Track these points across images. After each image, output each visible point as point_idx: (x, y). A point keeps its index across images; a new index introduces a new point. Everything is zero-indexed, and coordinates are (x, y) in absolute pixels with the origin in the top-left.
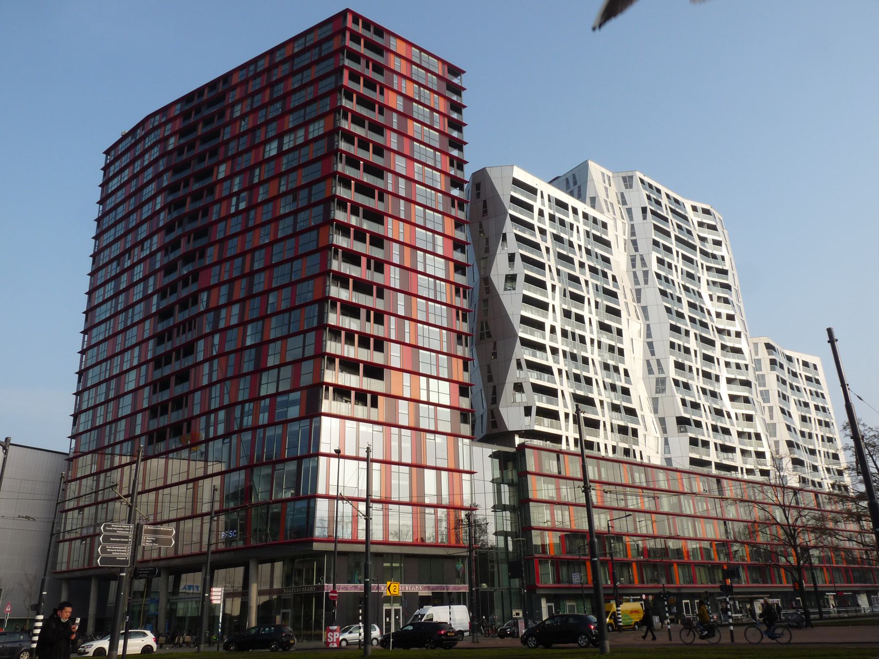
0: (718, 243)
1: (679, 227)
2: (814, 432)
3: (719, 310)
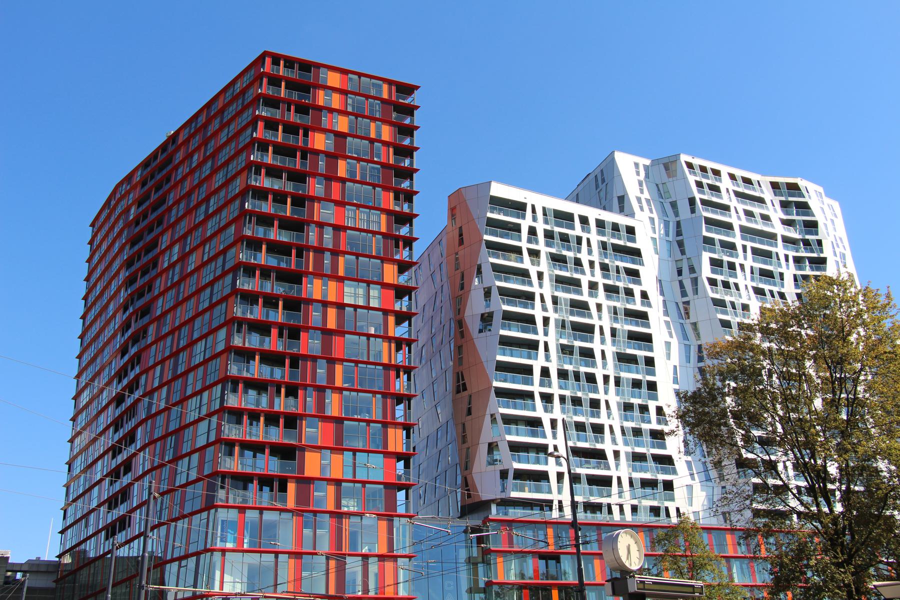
1: (749, 214)
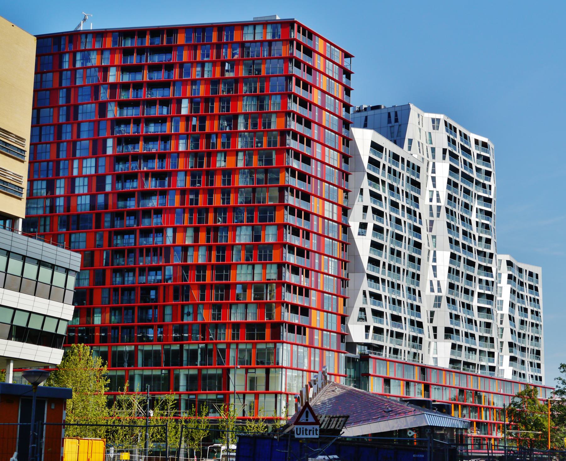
2: (527, 333)
3: (481, 235)
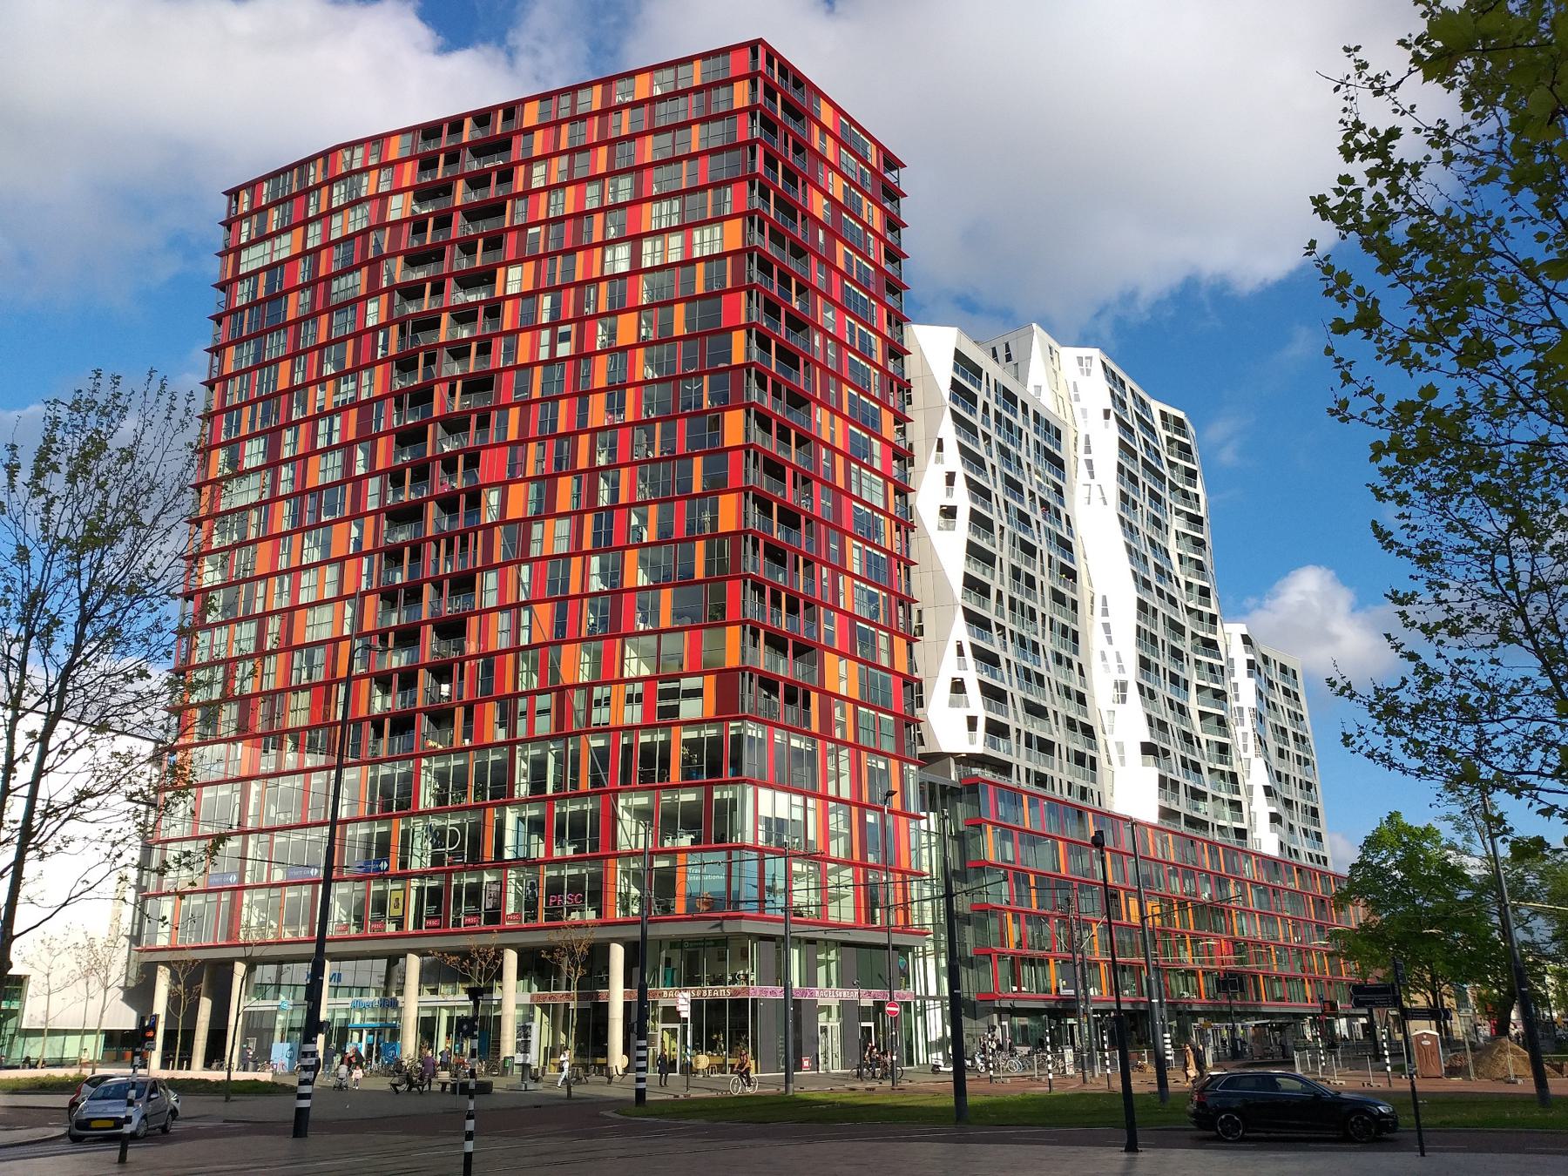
0: (1191, 474)
